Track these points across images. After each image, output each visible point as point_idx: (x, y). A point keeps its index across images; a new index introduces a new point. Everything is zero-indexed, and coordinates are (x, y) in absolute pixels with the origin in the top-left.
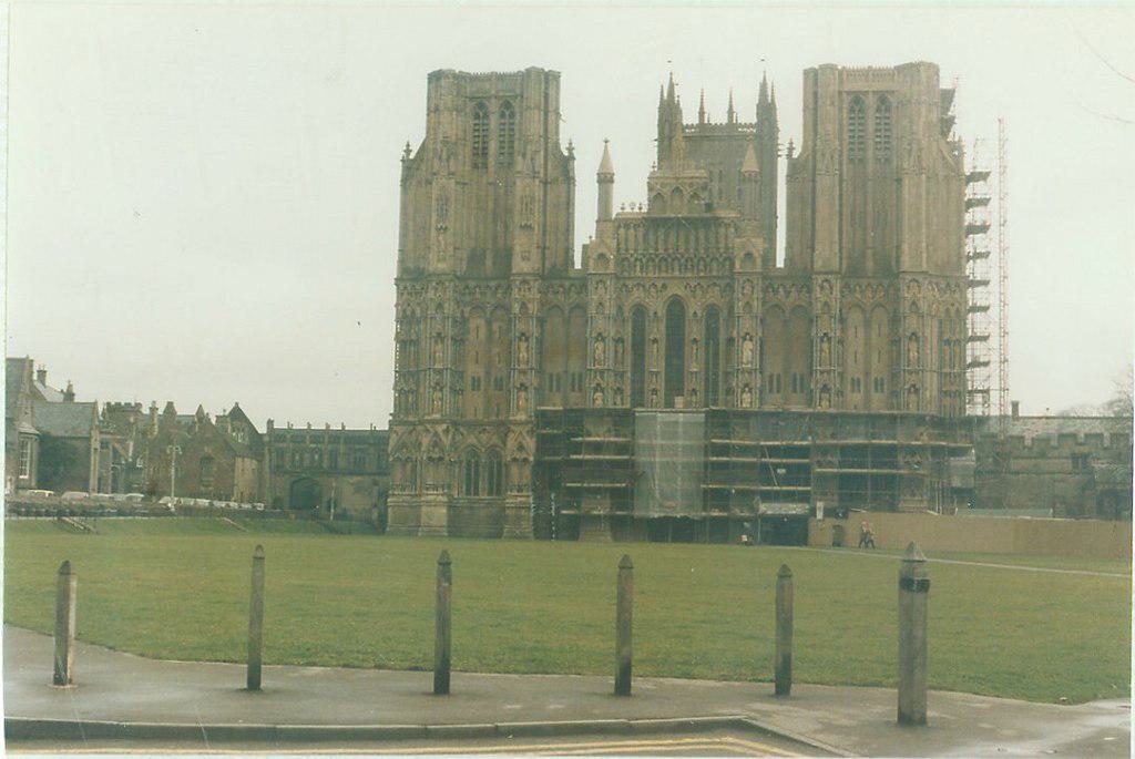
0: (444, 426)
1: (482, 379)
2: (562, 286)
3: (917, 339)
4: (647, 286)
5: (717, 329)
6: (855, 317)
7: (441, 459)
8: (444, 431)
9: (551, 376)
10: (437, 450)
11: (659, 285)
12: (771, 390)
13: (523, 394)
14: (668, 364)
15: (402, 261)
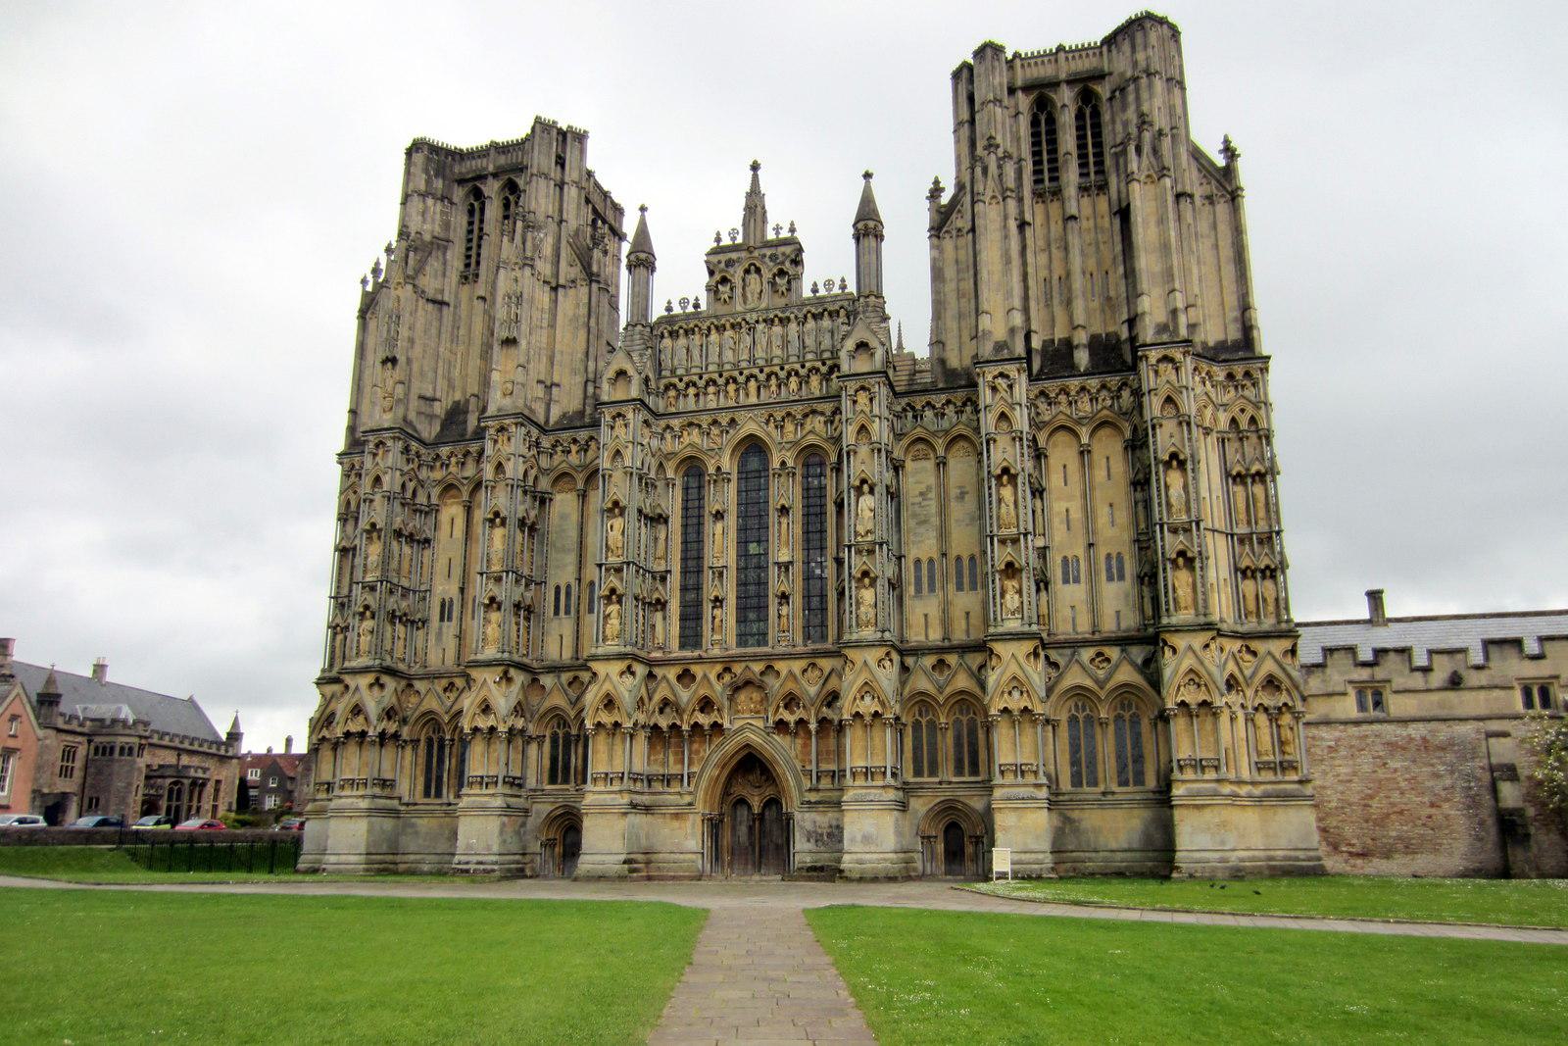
0: (370, 678)
1: (455, 602)
2: (575, 441)
3: (1182, 464)
4: (705, 426)
5: (822, 488)
6: (1062, 454)
7: (363, 734)
8: (371, 686)
9: (558, 589)
10: (361, 718)
11: (724, 423)
12: (919, 590)
13: (495, 616)
14: (743, 554)
15: (352, 429)
